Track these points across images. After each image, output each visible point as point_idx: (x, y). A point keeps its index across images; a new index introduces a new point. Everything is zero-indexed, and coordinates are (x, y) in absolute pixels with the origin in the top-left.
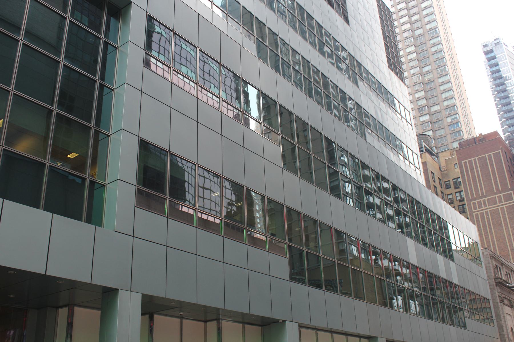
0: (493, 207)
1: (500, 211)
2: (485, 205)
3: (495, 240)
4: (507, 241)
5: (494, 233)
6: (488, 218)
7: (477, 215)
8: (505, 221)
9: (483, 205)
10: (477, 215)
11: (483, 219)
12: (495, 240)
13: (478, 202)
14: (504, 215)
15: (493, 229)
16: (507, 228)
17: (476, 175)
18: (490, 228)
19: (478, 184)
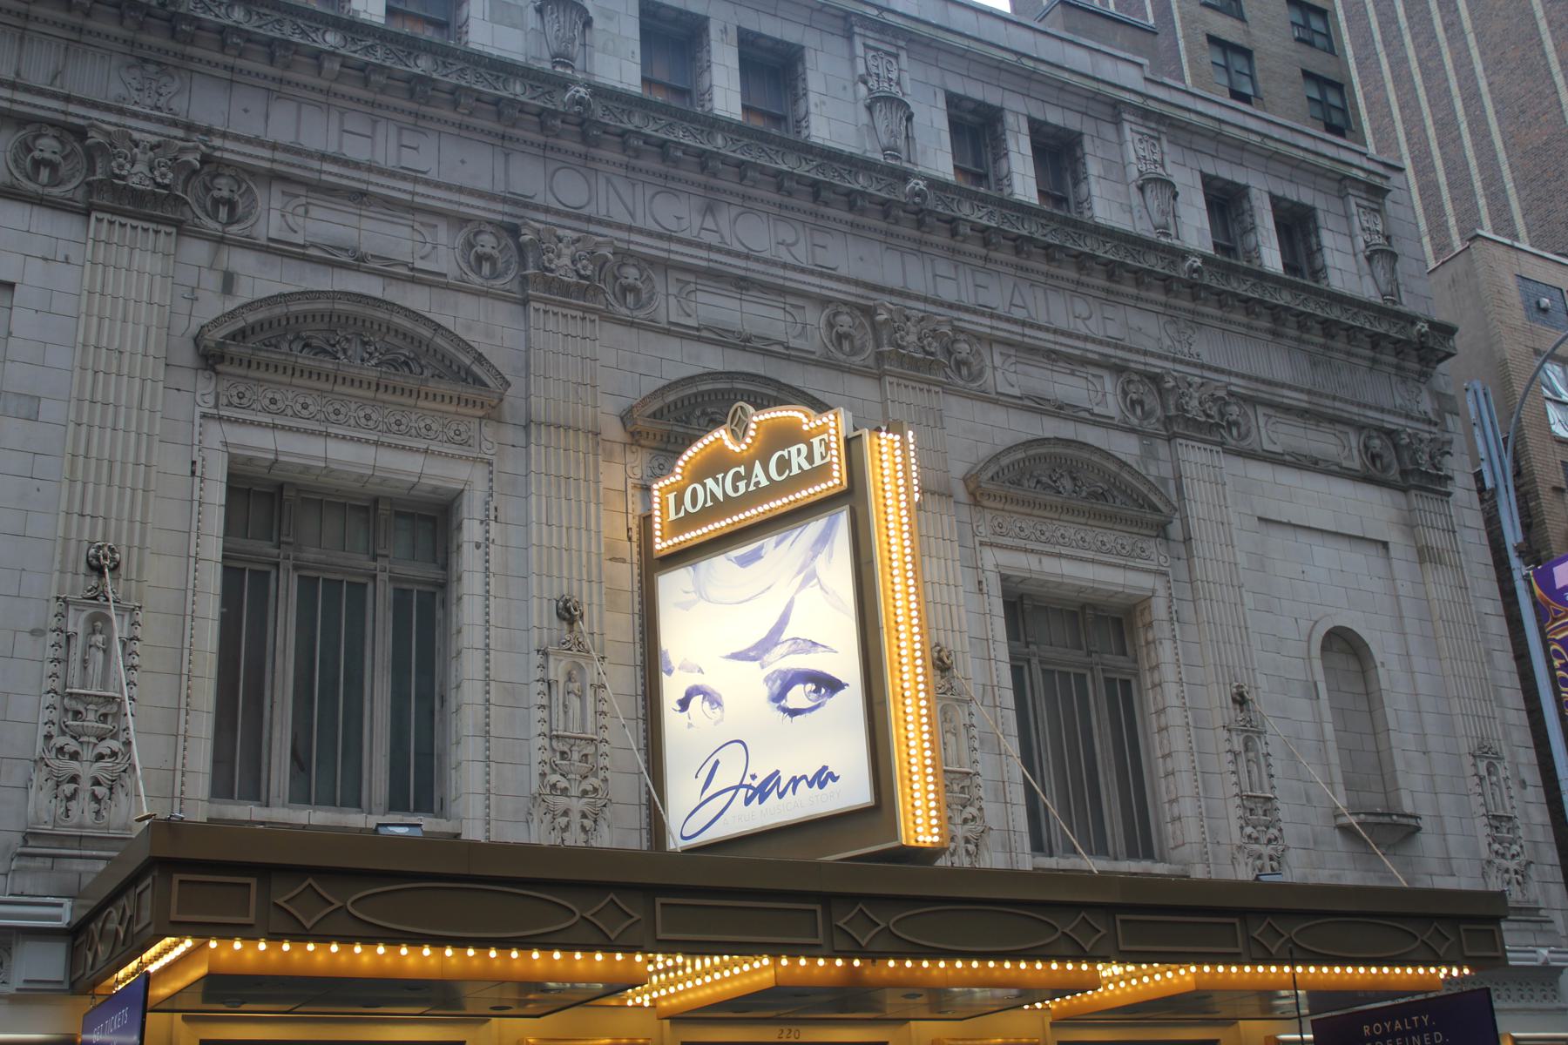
3: (1479, 68)
4: (1549, 45)
5: (1467, 24)
12: (1479, 68)
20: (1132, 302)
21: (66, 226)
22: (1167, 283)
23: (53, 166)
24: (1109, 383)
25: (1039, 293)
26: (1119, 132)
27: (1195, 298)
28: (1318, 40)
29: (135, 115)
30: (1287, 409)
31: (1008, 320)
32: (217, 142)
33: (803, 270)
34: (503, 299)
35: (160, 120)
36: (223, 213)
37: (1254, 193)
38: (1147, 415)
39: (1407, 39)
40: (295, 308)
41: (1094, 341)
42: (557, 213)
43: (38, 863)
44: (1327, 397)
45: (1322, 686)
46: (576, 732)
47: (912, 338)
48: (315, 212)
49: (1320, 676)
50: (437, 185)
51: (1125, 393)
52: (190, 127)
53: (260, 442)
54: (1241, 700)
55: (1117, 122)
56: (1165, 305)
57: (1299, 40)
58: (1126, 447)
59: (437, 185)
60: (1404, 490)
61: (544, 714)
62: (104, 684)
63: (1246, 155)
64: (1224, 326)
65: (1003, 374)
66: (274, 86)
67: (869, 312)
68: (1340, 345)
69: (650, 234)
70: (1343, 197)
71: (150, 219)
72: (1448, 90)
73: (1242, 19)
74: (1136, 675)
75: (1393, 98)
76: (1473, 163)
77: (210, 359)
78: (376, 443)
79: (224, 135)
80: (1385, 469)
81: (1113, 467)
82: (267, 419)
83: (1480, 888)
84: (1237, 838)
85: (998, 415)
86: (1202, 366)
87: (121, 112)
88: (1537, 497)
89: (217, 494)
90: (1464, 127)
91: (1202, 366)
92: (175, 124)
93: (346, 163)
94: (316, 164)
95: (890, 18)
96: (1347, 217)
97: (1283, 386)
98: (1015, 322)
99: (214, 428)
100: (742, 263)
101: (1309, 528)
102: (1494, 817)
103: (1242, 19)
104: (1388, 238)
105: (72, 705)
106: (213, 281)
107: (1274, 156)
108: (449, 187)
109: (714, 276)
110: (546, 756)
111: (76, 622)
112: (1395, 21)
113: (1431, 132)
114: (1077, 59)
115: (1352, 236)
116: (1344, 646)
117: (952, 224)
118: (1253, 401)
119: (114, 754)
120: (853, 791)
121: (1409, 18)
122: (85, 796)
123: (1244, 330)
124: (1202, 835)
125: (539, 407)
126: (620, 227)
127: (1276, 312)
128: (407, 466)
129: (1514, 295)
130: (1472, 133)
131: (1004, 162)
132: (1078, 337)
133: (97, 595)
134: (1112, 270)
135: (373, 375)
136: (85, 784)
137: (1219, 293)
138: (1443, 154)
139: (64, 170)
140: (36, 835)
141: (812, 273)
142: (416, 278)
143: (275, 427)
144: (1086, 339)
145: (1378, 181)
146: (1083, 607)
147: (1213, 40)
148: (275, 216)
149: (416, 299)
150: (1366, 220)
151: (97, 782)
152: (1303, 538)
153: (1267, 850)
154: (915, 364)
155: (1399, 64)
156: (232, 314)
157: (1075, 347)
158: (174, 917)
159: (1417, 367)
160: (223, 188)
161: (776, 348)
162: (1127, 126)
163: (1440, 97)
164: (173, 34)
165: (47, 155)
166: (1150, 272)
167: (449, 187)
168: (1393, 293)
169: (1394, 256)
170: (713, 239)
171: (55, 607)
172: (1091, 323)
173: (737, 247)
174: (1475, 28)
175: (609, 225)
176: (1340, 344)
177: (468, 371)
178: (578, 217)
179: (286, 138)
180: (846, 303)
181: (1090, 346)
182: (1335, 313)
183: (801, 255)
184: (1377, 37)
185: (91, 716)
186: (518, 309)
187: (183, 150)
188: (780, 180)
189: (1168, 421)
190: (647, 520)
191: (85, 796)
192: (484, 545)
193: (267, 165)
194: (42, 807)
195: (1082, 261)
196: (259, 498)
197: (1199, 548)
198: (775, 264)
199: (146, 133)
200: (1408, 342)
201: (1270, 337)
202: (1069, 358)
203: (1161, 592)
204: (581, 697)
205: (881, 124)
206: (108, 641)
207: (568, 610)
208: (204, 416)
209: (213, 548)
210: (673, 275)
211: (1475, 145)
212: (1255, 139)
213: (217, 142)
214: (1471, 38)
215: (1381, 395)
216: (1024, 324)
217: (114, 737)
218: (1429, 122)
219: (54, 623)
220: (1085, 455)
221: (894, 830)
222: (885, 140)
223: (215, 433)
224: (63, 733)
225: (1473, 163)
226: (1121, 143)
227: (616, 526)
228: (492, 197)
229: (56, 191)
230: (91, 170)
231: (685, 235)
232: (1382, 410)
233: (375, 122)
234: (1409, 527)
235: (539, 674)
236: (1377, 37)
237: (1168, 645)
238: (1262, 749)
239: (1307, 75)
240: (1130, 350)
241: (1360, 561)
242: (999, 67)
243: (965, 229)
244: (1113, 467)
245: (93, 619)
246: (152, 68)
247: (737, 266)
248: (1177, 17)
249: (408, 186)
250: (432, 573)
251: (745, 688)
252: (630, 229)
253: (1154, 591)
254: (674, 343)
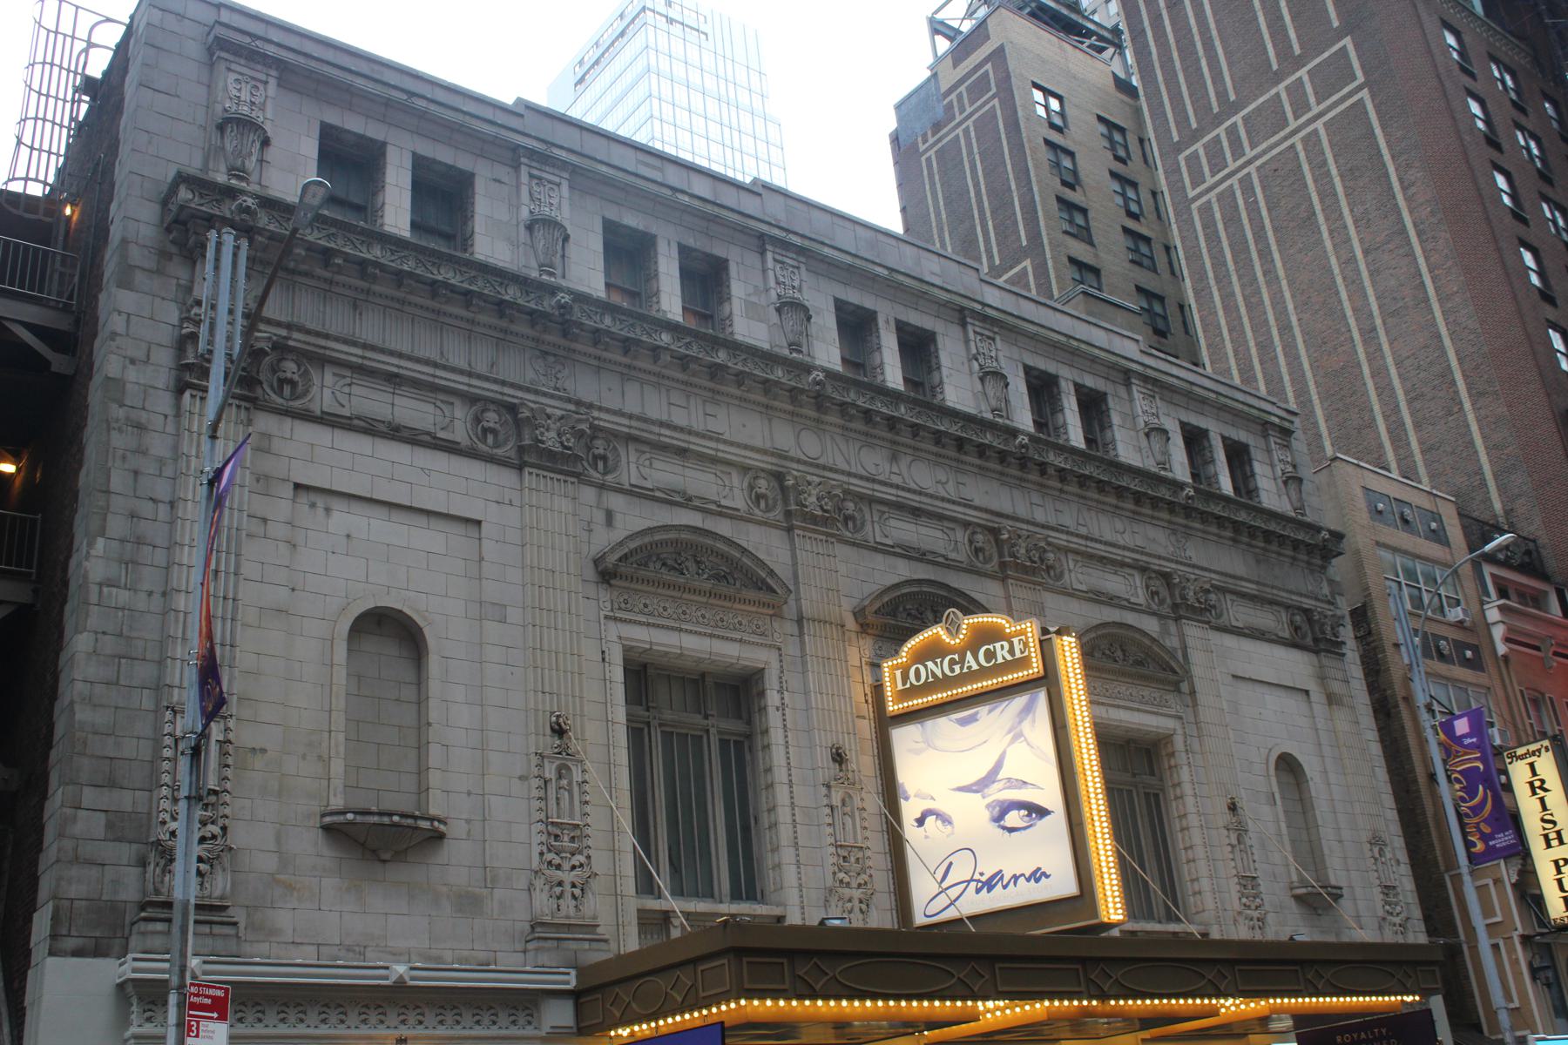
0: (1271, 148)
1: (1302, 155)
2: (1237, 151)
3: (1290, 307)
4: (1344, 295)
5: (1281, 273)
6: (1253, 208)
7: (1206, 210)
8: (1327, 194)
9: (1228, 155)
10: (1206, 210)
11: (1232, 219)
12: (1290, 307)
13: (1205, 147)
14: (1319, 166)
15: (1276, 256)
16: (1338, 231)
17: (1192, 21)
18: (1265, 254)
19: (1204, 63)
21: (507, 477)
22: (1171, 507)
23: (493, 431)
24: (1138, 580)
25: (1093, 514)
26: (1130, 392)
27: (1188, 517)
28: (1146, 262)
29: (545, 394)
30: (1243, 595)
31: (1077, 536)
32: (596, 414)
33: (954, 502)
34: (776, 527)
35: (560, 398)
36: (600, 465)
37: (1212, 434)
38: (1162, 602)
39: (1234, 279)
40: (657, 537)
41: (1129, 549)
42: (805, 463)
43: (549, 944)
45: (1277, 796)
46: (851, 842)
47: (1023, 551)
48: (657, 464)
49: (1275, 789)
50: (732, 444)
51: (1147, 587)
52: (578, 403)
53: (641, 636)
54: (1233, 808)
55: (1128, 385)
56: (1170, 522)
57: (1132, 261)
58: (1151, 625)
59: (732, 444)
60: (1317, 652)
61: (830, 830)
62: (572, 816)
65: (1079, 576)
66: (625, 371)
67: (995, 532)
69: (861, 478)
70: (1265, 436)
71: (561, 472)
72: (1266, 321)
73: (1092, 244)
74: (1162, 790)
75: (1223, 322)
76: (1286, 378)
77: (606, 575)
78: (711, 636)
79: (600, 409)
80: (1304, 637)
81: (1147, 642)
82: (643, 619)
83: (1378, 940)
84: (1237, 906)
85: (1075, 605)
86: (1194, 566)
87: (537, 392)
88: (1384, 651)
89: (618, 674)
90: (1279, 349)
91: (1194, 566)
92: (569, 400)
93: (675, 428)
94: (656, 429)
95: (990, 312)
96: (1269, 451)
97: (1242, 579)
98: (1081, 537)
99: (611, 624)
100: (917, 498)
103: (1092, 244)
104: (1294, 467)
105: (554, 831)
106: (600, 516)
107: (1223, 408)
108: (738, 445)
109: (899, 506)
110: (835, 860)
111: (550, 771)
112: (1225, 264)
113: (1253, 351)
114: (1099, 337)
115: (1272, 466)
116: (1288, 765)
117: (1043, 468)
118: (1223, 590)
119: (581, 865)
120: (1062, 884)
121: (1236, 263)
122: (568, 895)
124: (1216, 908)
125: (807, 608)
126: (843, 472)
128: (730, 652)
129: (1361, 503)
130: (1285, 355)
131: (1060, 416)
132: (1119, 547)
133: (563, 751)
134: (1138, 498)
135: (708, 586)
136: (568, 887)
137: (1202, 513)
138: (1263, 370)
139: (501, 437)
140: (543, 924)
141: (959, 504)
142: (723, 513)
143: (648, 625)
144: (1124, 548)
145: (1286, 424)
146: (1129, 741)
147: (1072, 260)
148: (633, 467)
149: (724, 528)
150: (1278, 454)
151: (574, 886)
152: (1260, 689)
153: (1256, 914)
154: (1025, 570)
155: (1228, 297)
156: (621, 544)
157: (1117, 554)
158: (747, 986)
160: (600, 447)
161: (941, 560)
162: (1134, 388)
163: (1260, 325)
164: (565, 334)
165: (491, 425)
166: (1162, 499)
167: (738, 445)
168: (1300, 509)
169: (1300, 480)
170: (896, 480)
171: (535, 760)
172: (1126, 536)
173: (913, 486)
174: (1287, 277)
175: (836, 471)
176: (1274, 547)
177: (763, 581)
178: (817, 466)
179: (636, 410)
180: (979, 525)
181: (1127, 554)
182: (1272, 526)
183: (951, 491)
184: (1211, 275)
185: (566, 838)
186: (784, 533)
187: (580, 421)
188: (938, 437)
189: (1175, 606)
190: (878, 689)
191: (568, 895)
192: (782, 707)
193: (626, 430)
194: (543, 903)
195: (1120, 492)
196: (642, 676)
197: (1201, 698)
198: (937, 498)
199: (556, 408)
200: (1316, 546)
202: (1113, 562)
203: (1180, 731)
204: (853, 817)
205: (991, 393)
206: (570, 784)
207: (839, 755)
208: (606, 617)
209: (620, 714)
210: (876, 507)
211: (1288, 364)
212: (1213, 396)
213: (596, 414)
214: (1284, 283)
215: (1296, 583)
216: (1087, 538)
217: (581, 853)
218: (1252, 344)
219: (535, 771)
220: (1131, 634)
221: (1094, 911)
222: (994, 403)
223: (614, 630)
224: (549, 851)
225: (1286, 378)
226: (1131, 400)
227: (859, 692)
228: (764, 452)
229: (499, 452)
230: (520, 436)
231: (881, 478)
232: (1301, 595)
233: (688, 397)
234: (1322, 679)
235: (825, 801)
236: (1211, 275)
237: (1185, 768)
238: (1249, 842)
239: (1139, 289)
240: (1150, 555)
241: (1293, 703)
242: (1055, 346)
243: (1051, 471)
244: (1147, 642)
245: (559, 770)
246: (551, 359)
247: (914, 500)
248: (1046, 241)
249: (713, 444)
250: (734, 726)
251: (972, 813)
252: (849, 474)
254: (879, 557)
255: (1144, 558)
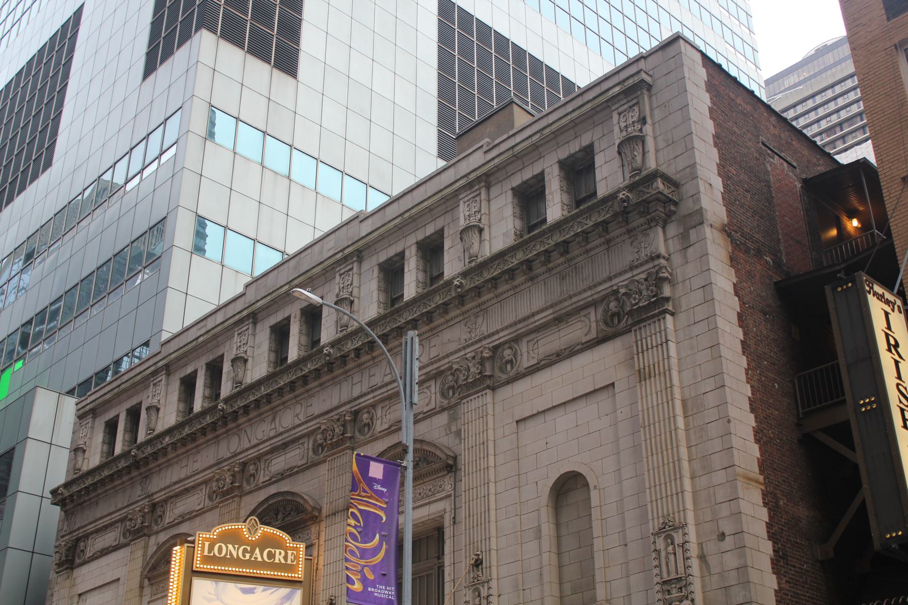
20: (446, 326)
44: (565, 300)
54: (478, 563)
63: (541, 149)
64: (499, 299)
68: (576, 252)
101: (554, 407)
102: (665, 582)
123: (512, 292)
127: (528, 263)
159: (642, 220)
201: (530, 283)
241: (587, 411)
242: (399, 228)
253: (445, 510)
255: (435, 366)
